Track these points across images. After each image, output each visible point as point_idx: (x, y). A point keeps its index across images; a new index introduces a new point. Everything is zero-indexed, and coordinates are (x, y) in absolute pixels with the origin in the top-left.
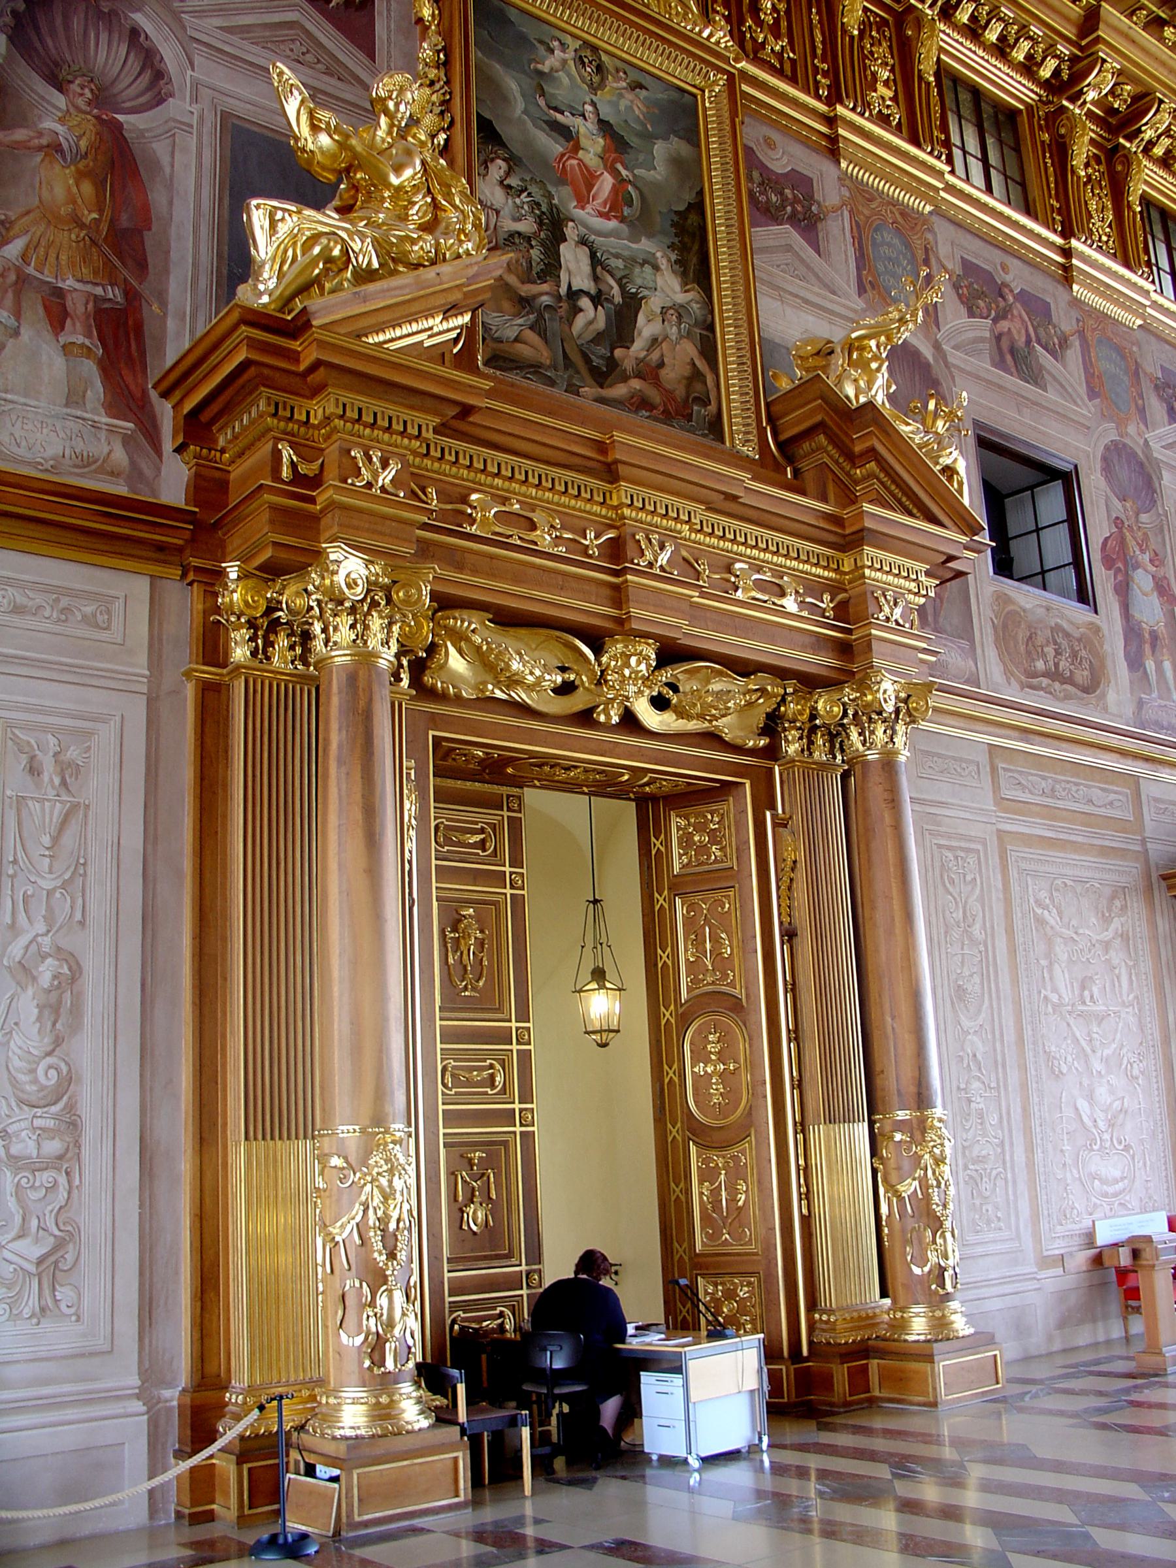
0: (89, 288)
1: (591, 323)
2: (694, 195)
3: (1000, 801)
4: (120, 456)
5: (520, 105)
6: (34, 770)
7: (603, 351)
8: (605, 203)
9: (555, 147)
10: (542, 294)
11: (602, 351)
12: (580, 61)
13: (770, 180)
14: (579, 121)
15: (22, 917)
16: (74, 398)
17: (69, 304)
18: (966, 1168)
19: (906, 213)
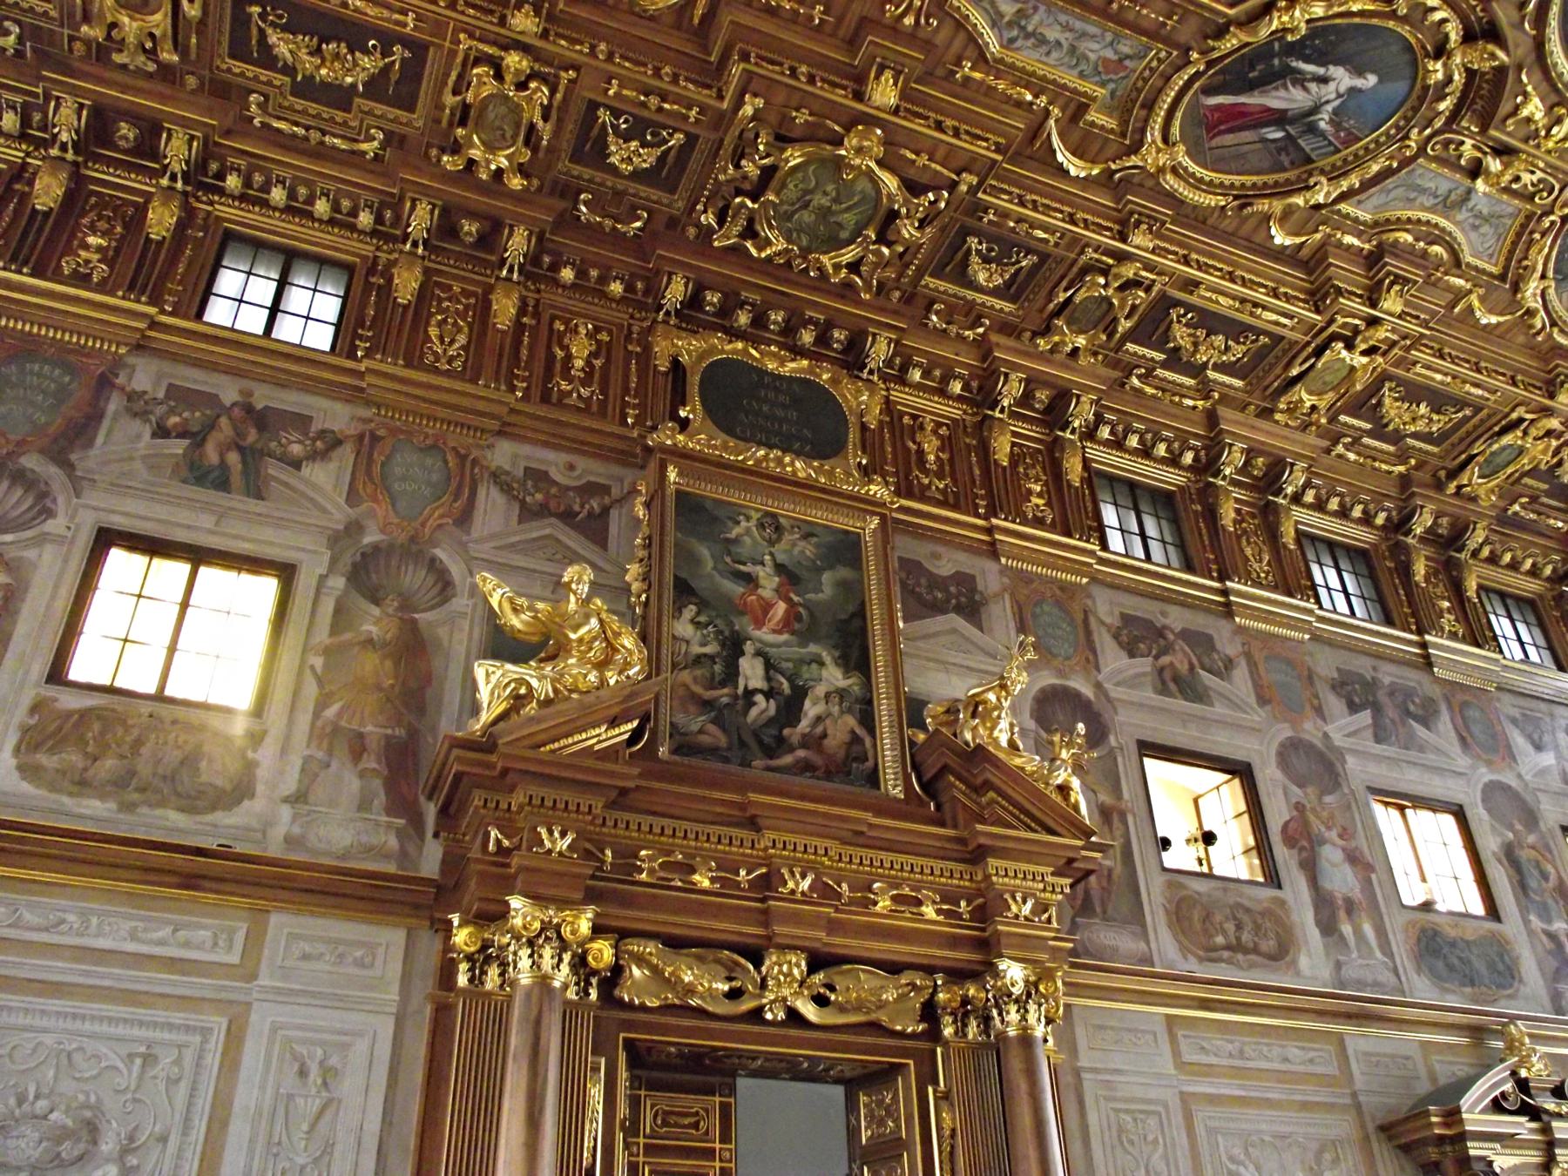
0: (382, 731)
1: (763, 712)
3: (1181, 1065)
4: (393, 842)
5: (710, 564)
6: (303, 1073)
9: (736, 589)
11: (774, 732)
12: (761, 526)
13: (936, 582)
14: (759, 568)
16: (364, 805)
17: (367, 741)
19: (1064, 587)
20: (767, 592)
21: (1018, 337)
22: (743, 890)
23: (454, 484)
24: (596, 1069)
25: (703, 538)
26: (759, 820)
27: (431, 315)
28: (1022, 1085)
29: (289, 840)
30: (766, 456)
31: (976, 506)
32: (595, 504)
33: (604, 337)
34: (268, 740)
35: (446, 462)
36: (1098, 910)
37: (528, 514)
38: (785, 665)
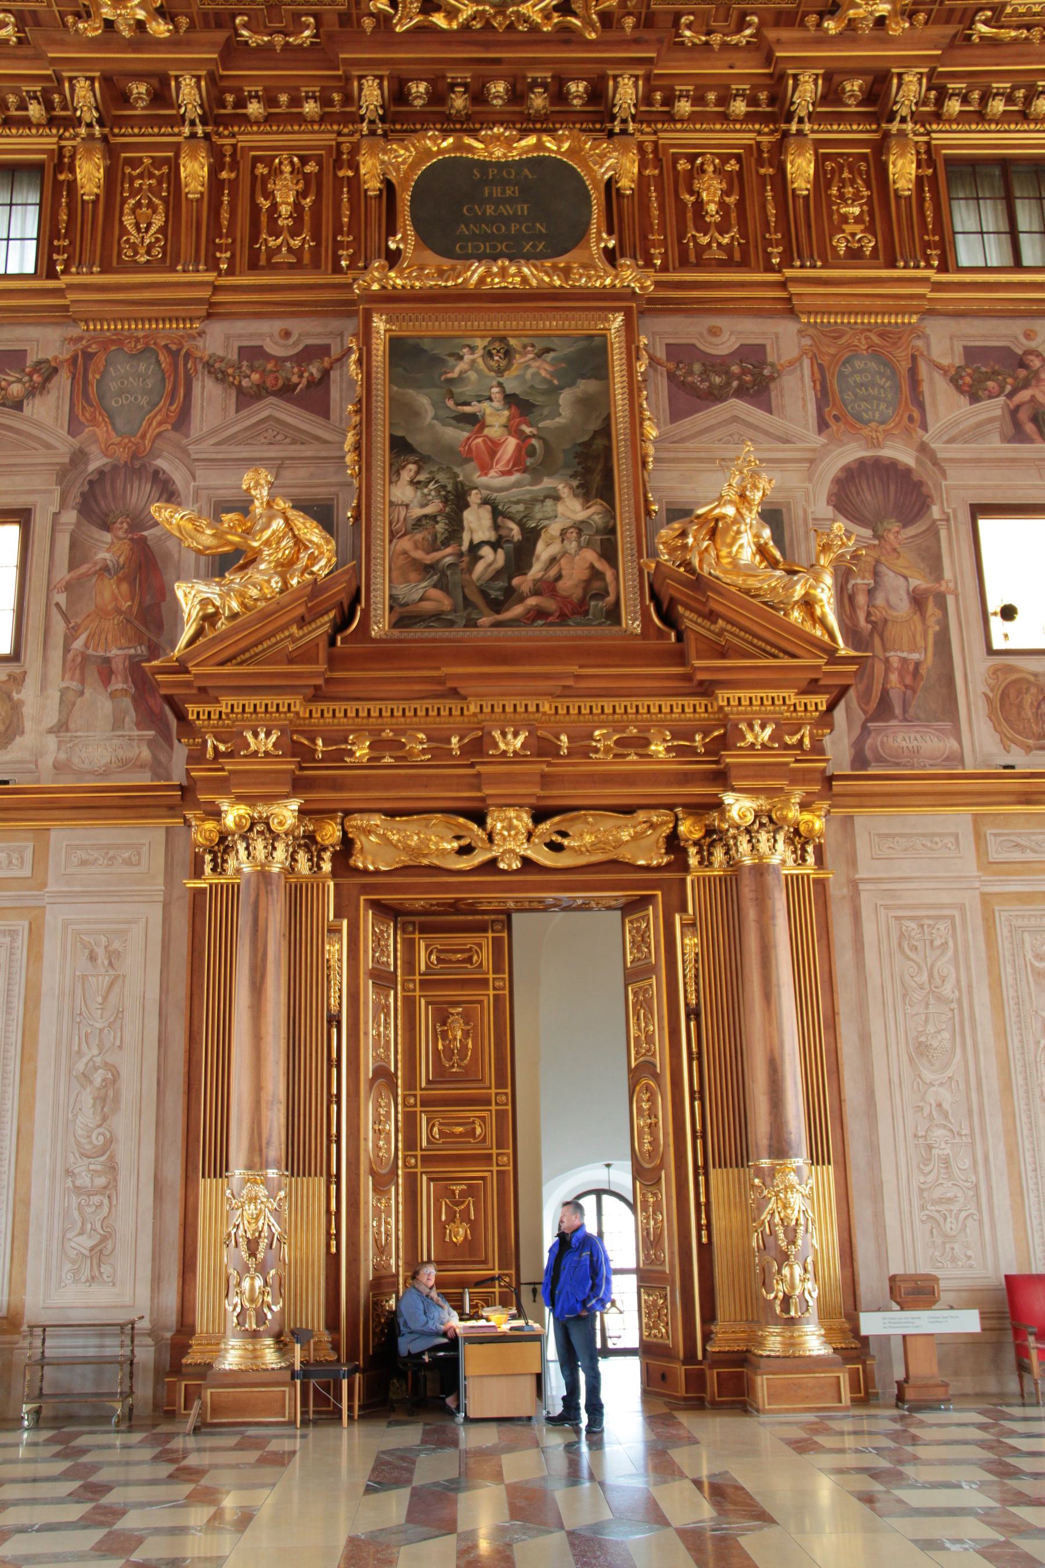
0: (126, 652)
1: (490, 565)
2: (600, 421)
3: (986, 865)
4: (146, 754)
5: (431, 413)
6: (92, 958)
8: (508, 462)
10: (444, 557)
11: (501, 584)
13: (714, 364)
14: (486, 405)
15: (84, 1046)
16: (117, 724)
17: (114, 666)
18: (923, 1208)
20: (495, 430)
21: (802, 24)
22: (454, 757)
23: (169, 387)
24: (335, 931)
25: (418, 386)
27: (124, 201)
28: (751, 914)
29: (58, 767)
30: (489, 273)
31: (768, 256)
32: (314, 370)
33: (311, 168)
34: (28, 680)
35: (158, 362)
36: (898, 711)
37: (246, 398)
38: (514, 509)
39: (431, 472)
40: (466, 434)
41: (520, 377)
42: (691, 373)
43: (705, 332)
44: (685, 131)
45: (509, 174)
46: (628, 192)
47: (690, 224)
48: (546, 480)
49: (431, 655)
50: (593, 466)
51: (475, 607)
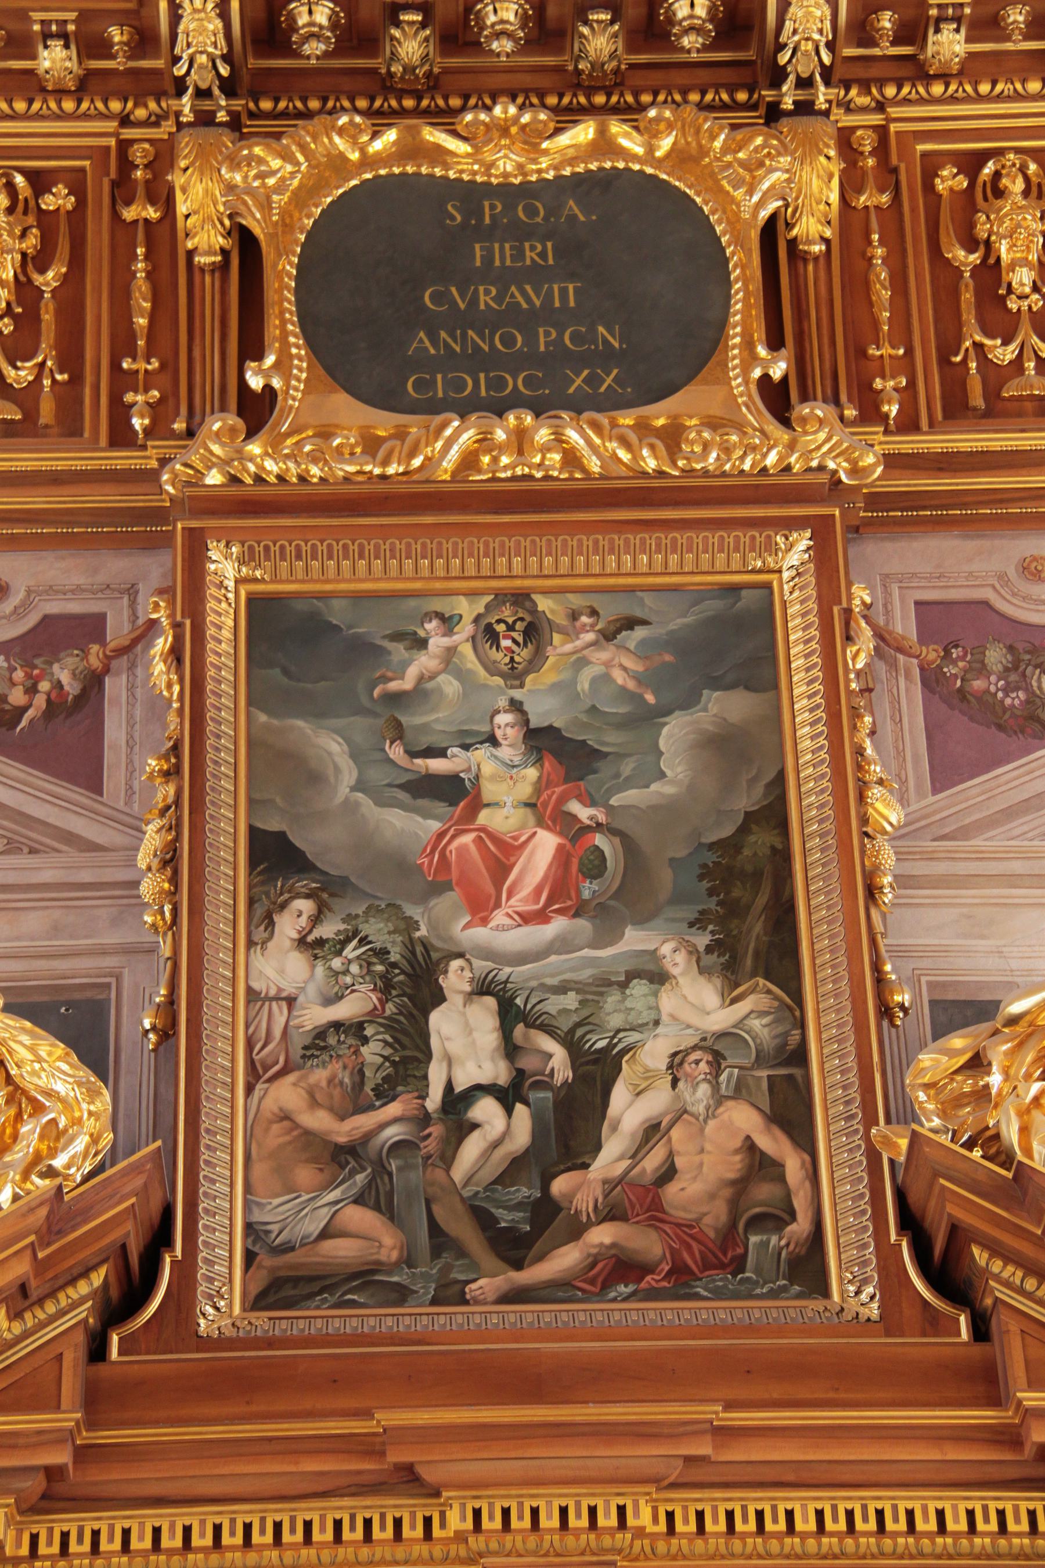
1: (496, 1144)
2: (759, 790)
5: (349, 774)
7: (525, 1191)
8: (538, 891)
11: (524, 1192)
14: (481, 754)
20: (503, 817)
25: (319, 711)
26: (420, 1470)
30: (484, 441)
33: (57, 200)
38: (554, 1004)
39: (349, 918)
40: (435, 825)
41: (566, 689)
42: (981, 669)
43: (1012, 573)
44: (953, 100)
45: (531, 212)
46: (817, 248)
47: (969, 317)
48: (630, 932)
49: (350, 1378)
50: (746, 898)
51: (461, 1253)
